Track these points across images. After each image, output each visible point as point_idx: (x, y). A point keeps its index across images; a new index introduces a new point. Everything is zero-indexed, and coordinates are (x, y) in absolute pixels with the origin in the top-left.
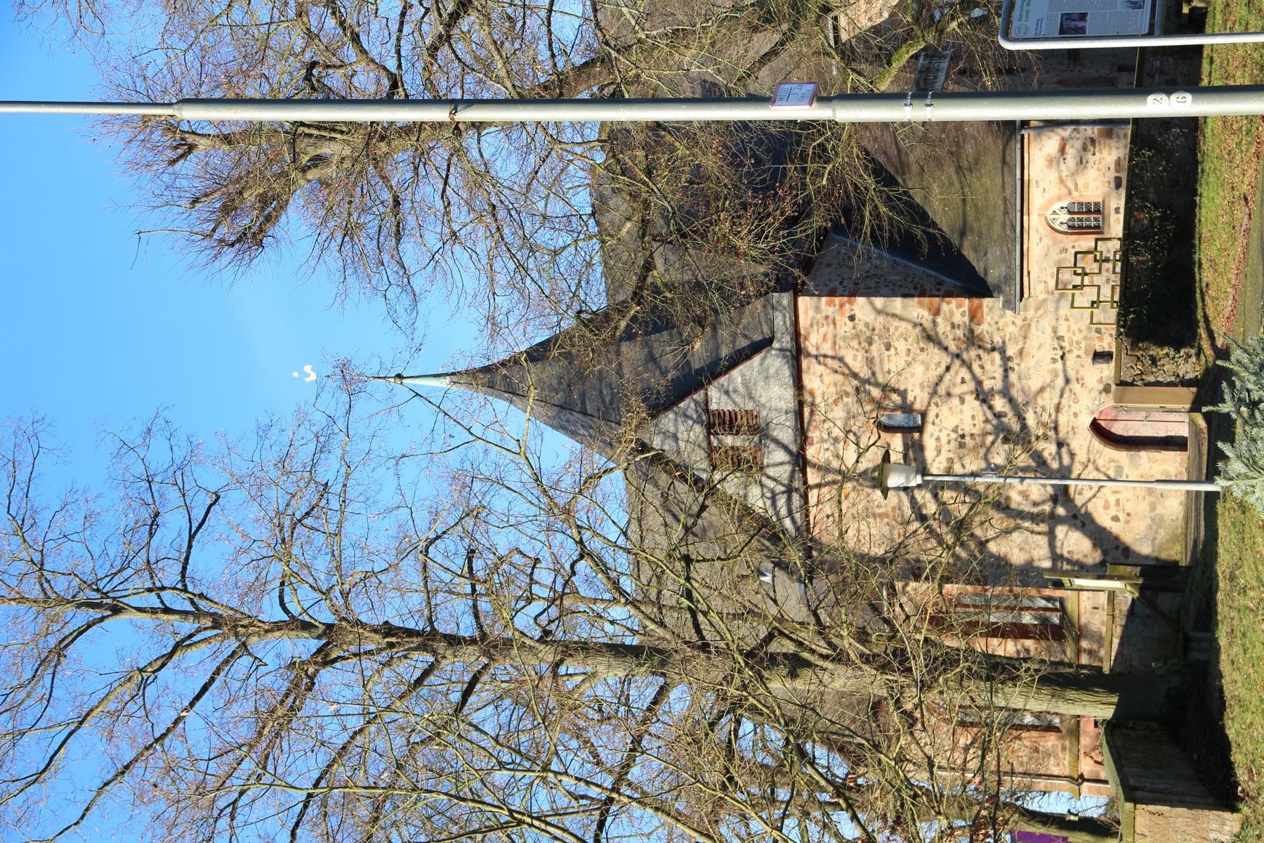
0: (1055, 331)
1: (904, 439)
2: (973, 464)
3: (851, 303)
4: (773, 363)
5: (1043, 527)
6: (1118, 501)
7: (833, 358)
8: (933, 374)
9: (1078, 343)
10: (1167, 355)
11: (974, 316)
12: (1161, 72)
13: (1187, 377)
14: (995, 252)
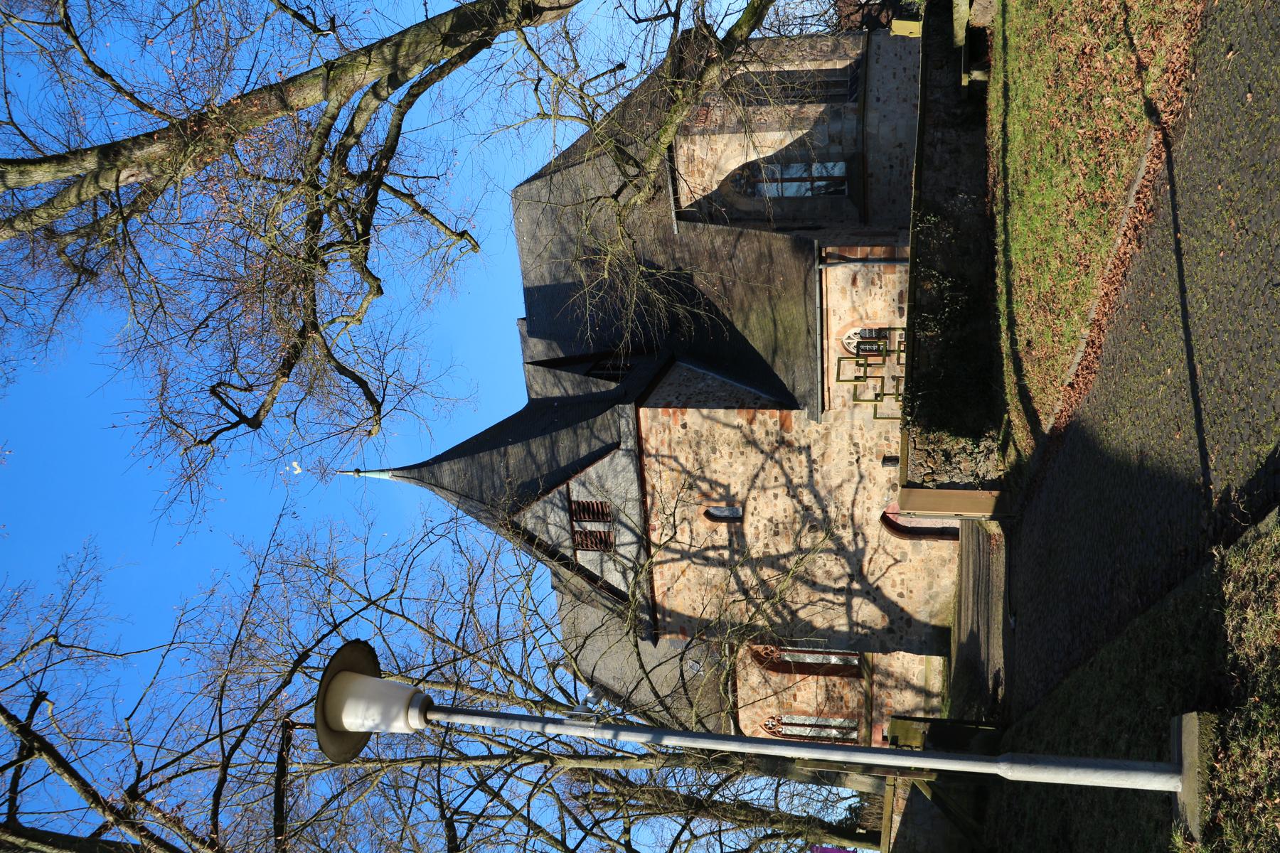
0: (851, 437)
1: (729, 528)
2: (785, 548)
3: (683, 414)
4: (621, 461)
5: (842, 599)
6: (903, 581)
7: (670, 457)
8: (751, 471)
10: (964, 449)
11: (784, 425)
12: (943, 142)
13: (988, 478)
14: (800, 372)
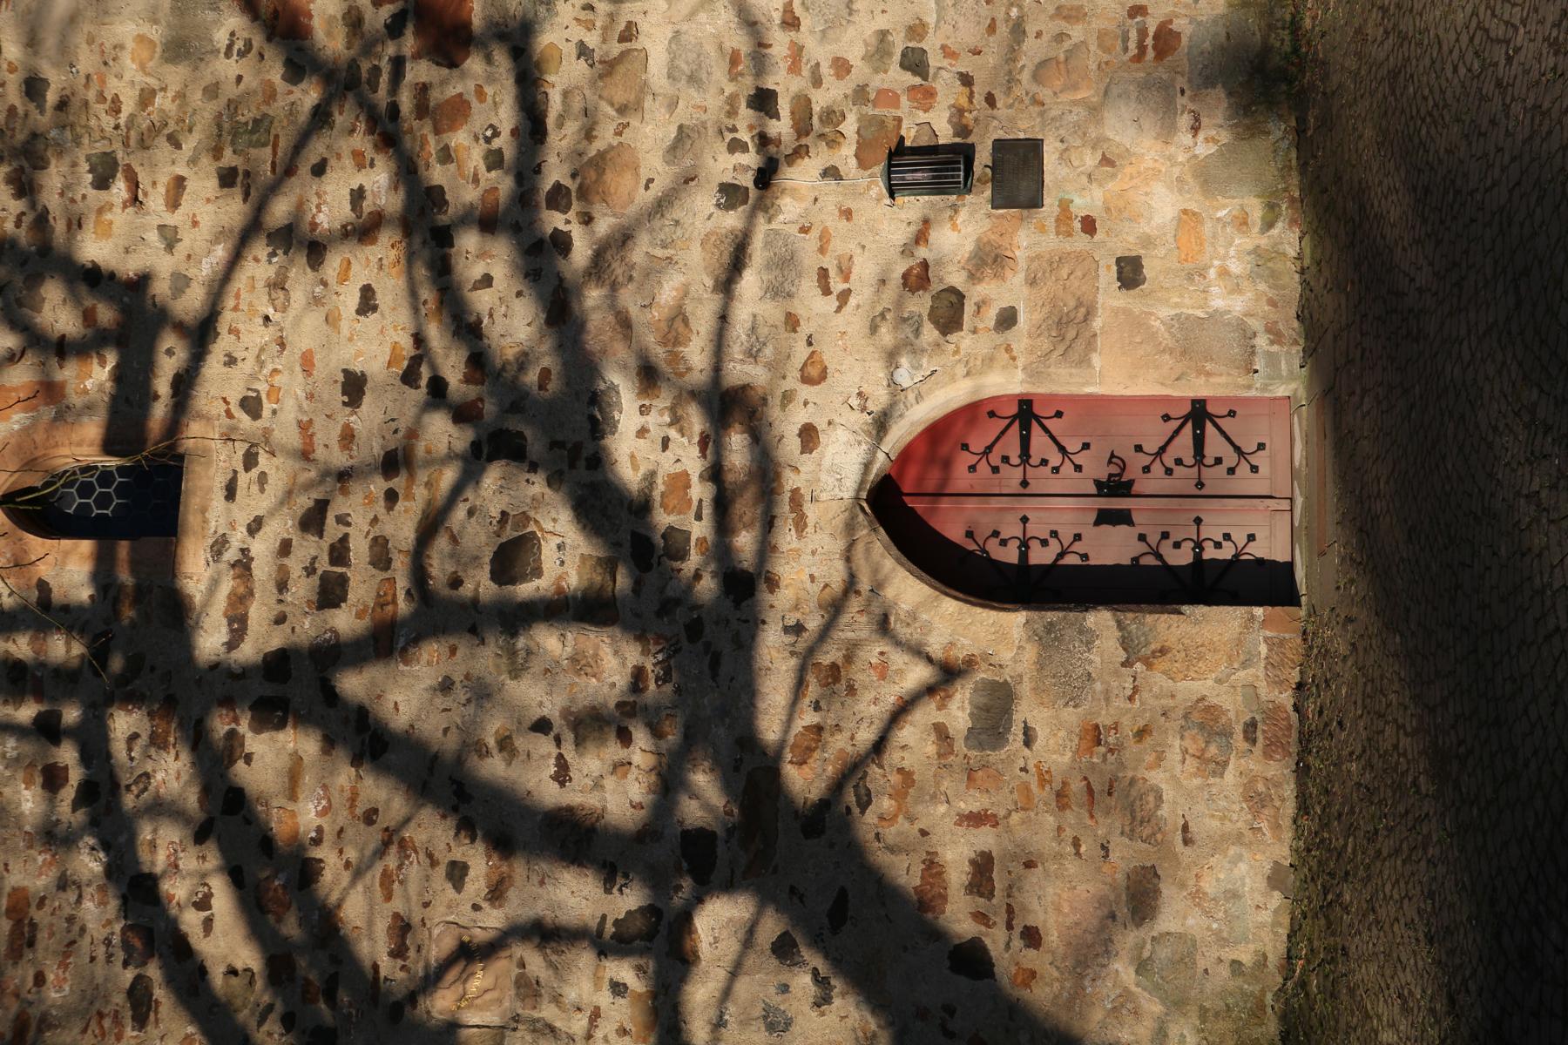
6: (982, 866)
9: (832, 116)
